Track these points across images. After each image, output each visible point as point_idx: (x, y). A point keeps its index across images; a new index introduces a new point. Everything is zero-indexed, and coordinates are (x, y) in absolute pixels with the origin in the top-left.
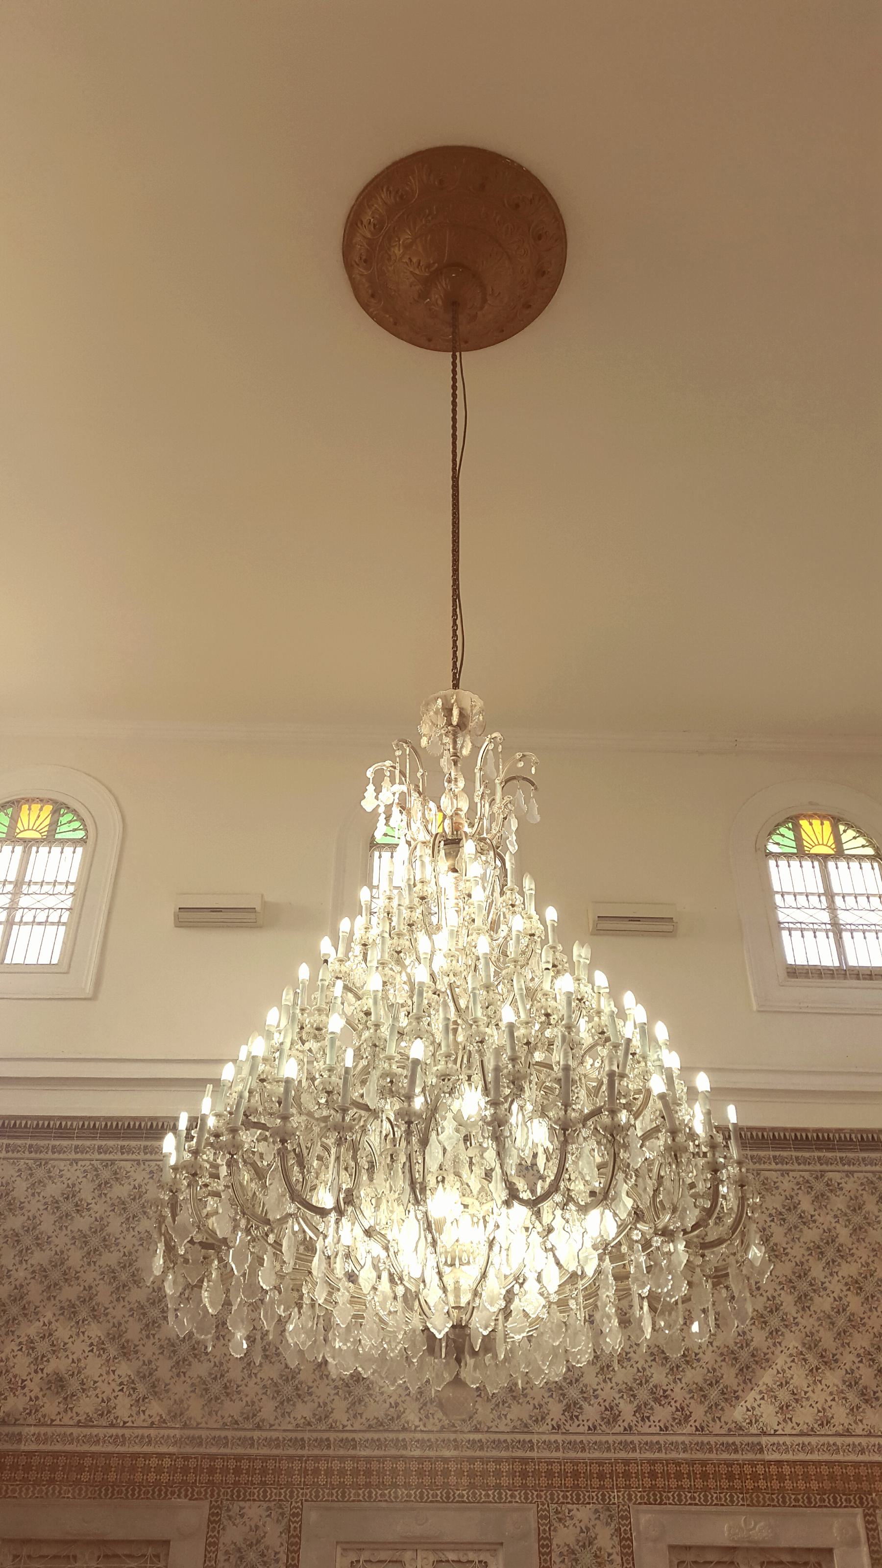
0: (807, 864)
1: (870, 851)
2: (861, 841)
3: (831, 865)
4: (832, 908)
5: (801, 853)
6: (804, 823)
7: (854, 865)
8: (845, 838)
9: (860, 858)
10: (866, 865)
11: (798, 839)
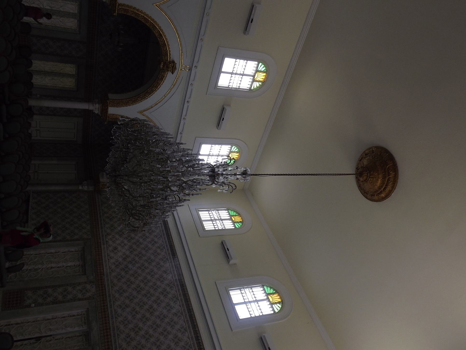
0: (254, 72)
1: (252, 88)
2: (255, 87)
3: (252, 78)
4: (240, 74)
5: (257, 71)
6: (265, 74)
7: (250, 83)
8: (257, 83)
9: (251, 85)
10: (249, 86)
11: (261, 71)
